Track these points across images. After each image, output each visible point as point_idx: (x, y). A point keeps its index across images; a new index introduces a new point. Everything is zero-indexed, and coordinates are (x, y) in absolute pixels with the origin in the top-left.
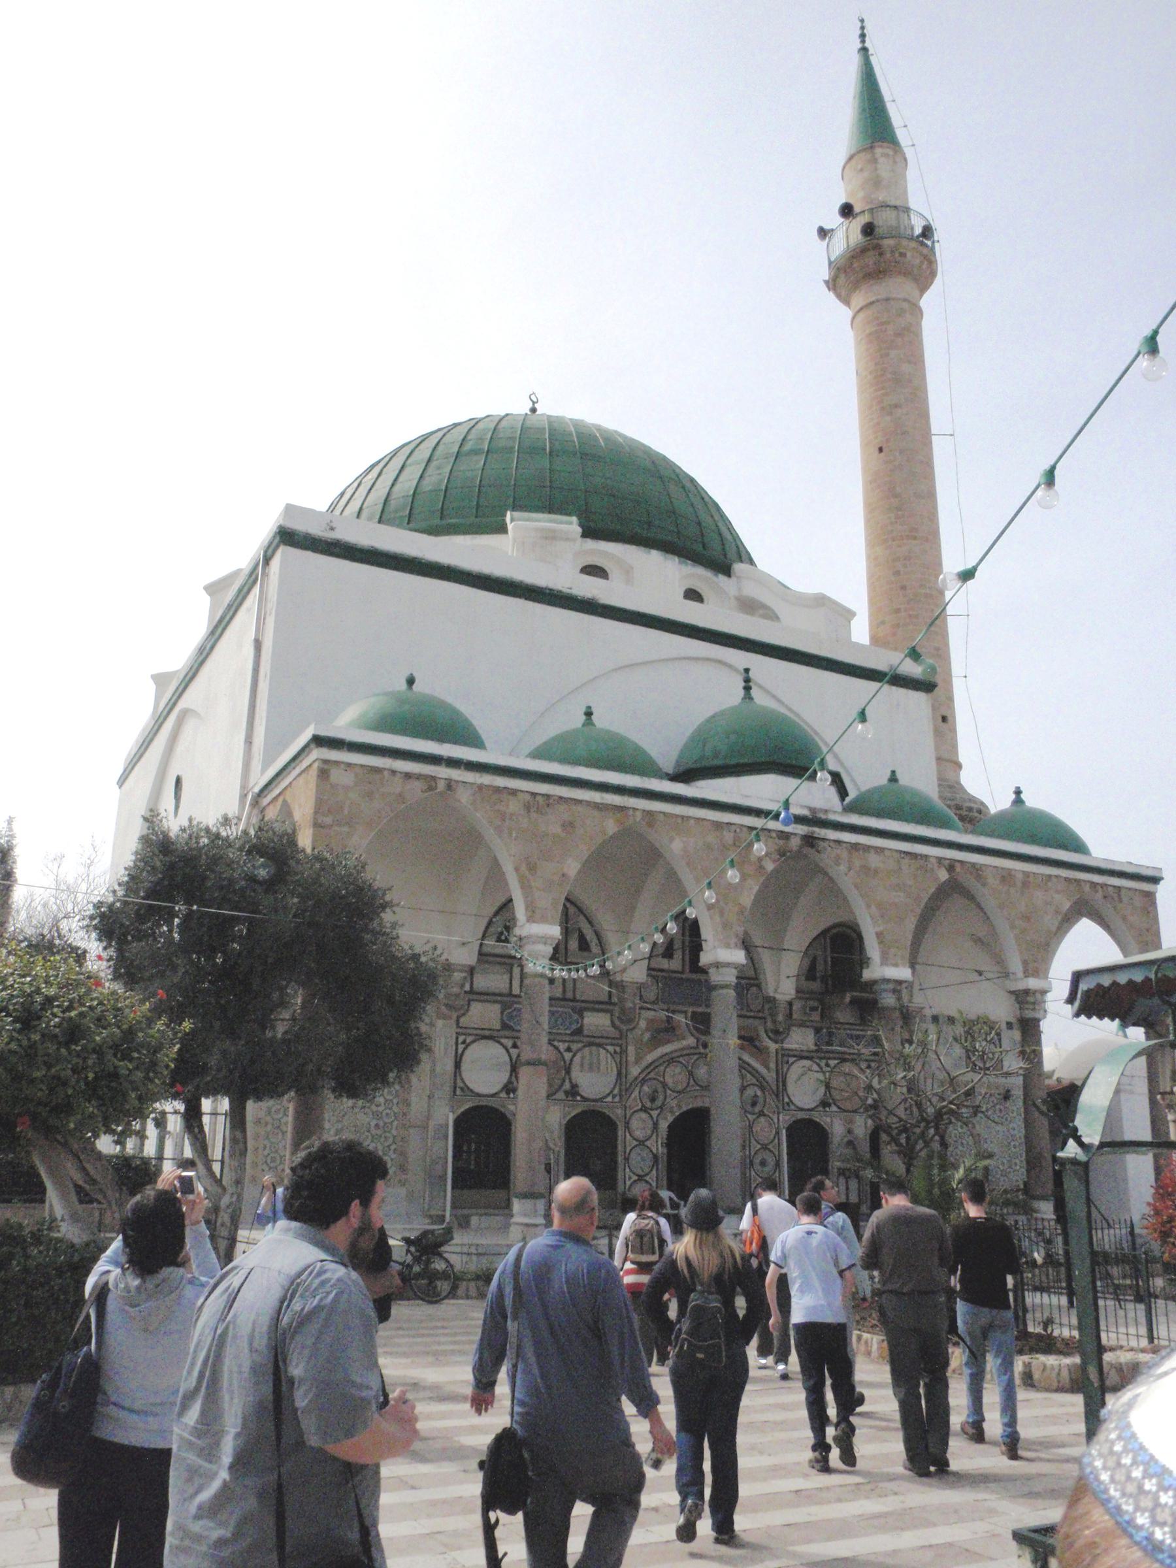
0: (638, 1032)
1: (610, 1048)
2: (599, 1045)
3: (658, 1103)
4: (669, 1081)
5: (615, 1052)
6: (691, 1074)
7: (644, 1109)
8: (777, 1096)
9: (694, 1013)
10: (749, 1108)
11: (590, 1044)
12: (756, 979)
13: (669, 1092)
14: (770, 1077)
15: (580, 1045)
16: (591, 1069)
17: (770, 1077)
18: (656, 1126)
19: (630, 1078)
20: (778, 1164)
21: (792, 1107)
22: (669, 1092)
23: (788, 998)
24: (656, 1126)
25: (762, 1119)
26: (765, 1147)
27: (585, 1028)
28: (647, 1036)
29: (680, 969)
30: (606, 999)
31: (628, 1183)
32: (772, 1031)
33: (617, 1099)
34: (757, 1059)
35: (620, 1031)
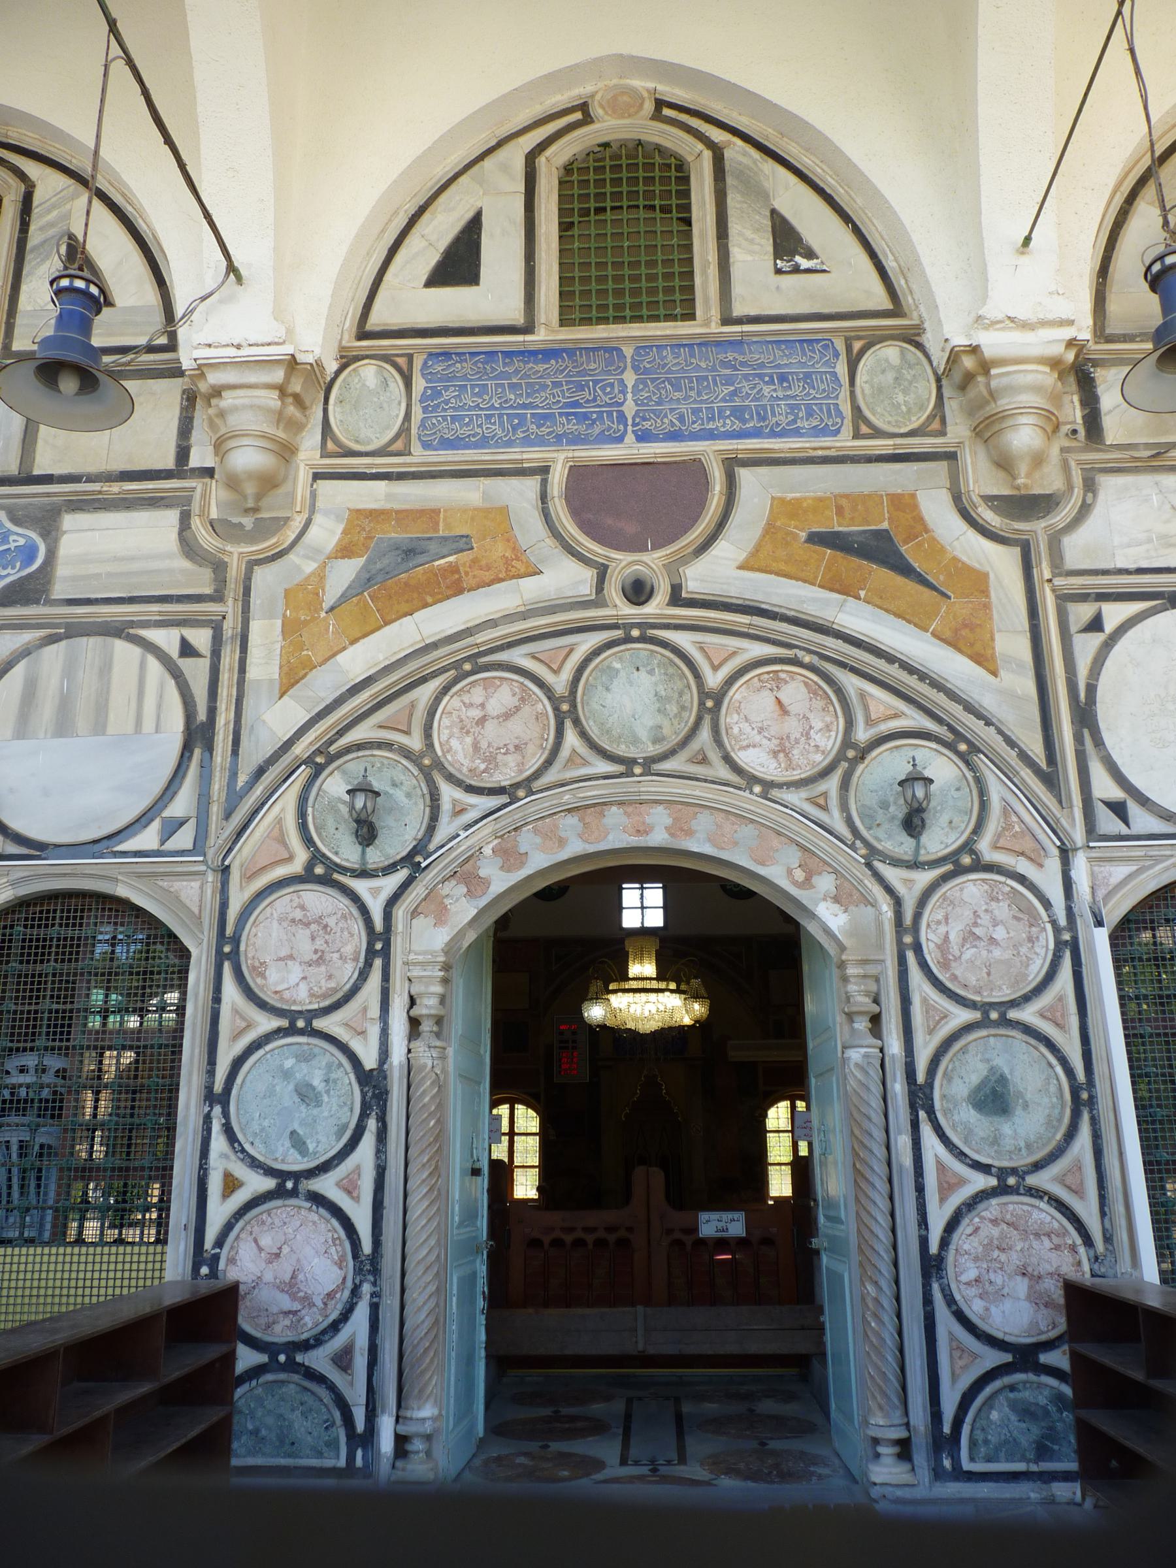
0: (302, 564)
1: (167, 639)
2: (118, 630)
3: (396, 840)
4: (457, 751)
5: (187, 650)
6: (566, 711)
7: (322, 873)
8: (1051, 779)
9: (578, 474)
10: (899, 844)
11: (74, 631)
12: (897, 310)
13: (448, 793)
14: (1004, 693)
15: (28, 636)
16: (63, 727)
17: (1004, 693)
18: (379, 944)
19: (255, 750)
20: (1083, 1098)
21: (1142, 821)
22: (448, 793)
23: (1051, 341)
24: (379, 944)
25: (971, 889)
26: (995, 1016)
27: (62, 570)
28: (345, 572)
29: (518, 318)
30: (169, 463)
31: (218, 1212)
32: (988, 499)
33: (184, 839)
34: (916, 619)
35: (219, 568)
